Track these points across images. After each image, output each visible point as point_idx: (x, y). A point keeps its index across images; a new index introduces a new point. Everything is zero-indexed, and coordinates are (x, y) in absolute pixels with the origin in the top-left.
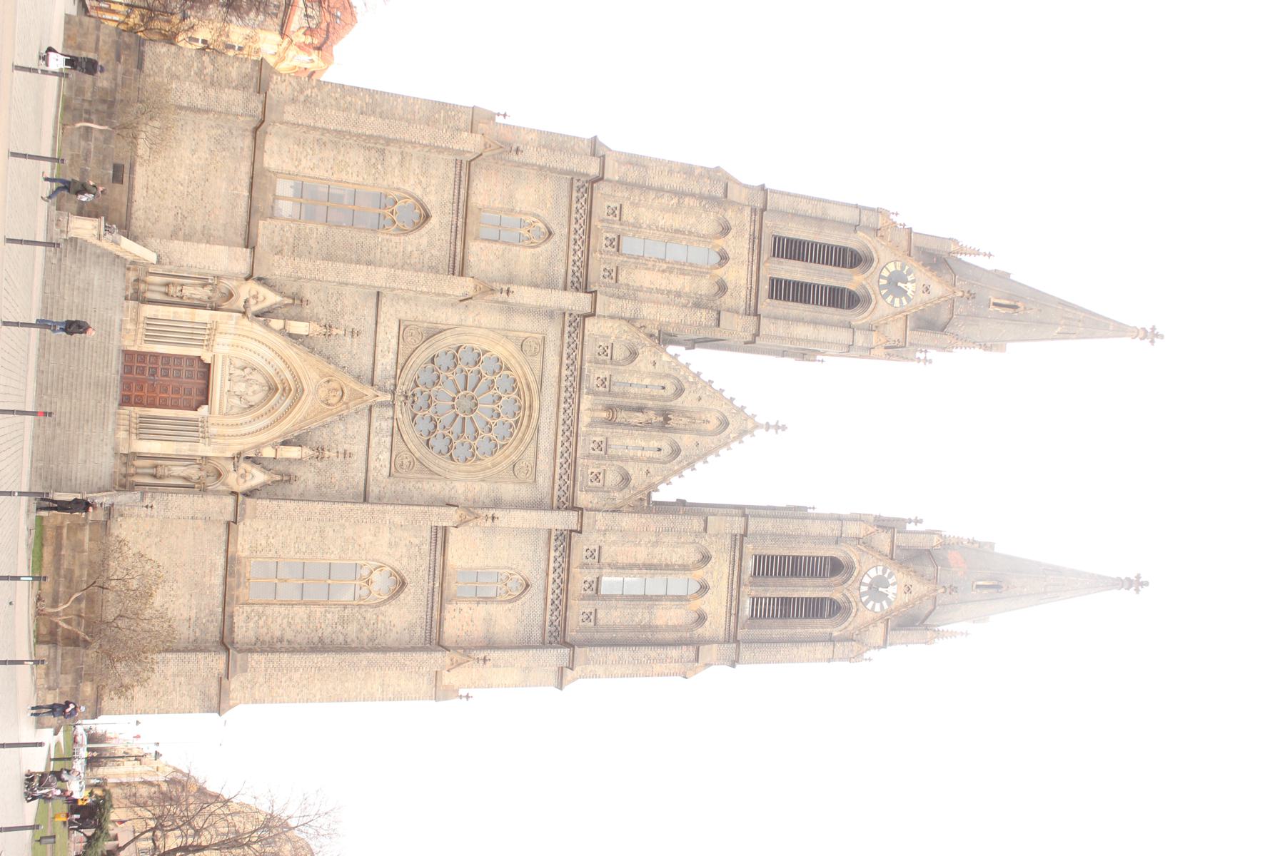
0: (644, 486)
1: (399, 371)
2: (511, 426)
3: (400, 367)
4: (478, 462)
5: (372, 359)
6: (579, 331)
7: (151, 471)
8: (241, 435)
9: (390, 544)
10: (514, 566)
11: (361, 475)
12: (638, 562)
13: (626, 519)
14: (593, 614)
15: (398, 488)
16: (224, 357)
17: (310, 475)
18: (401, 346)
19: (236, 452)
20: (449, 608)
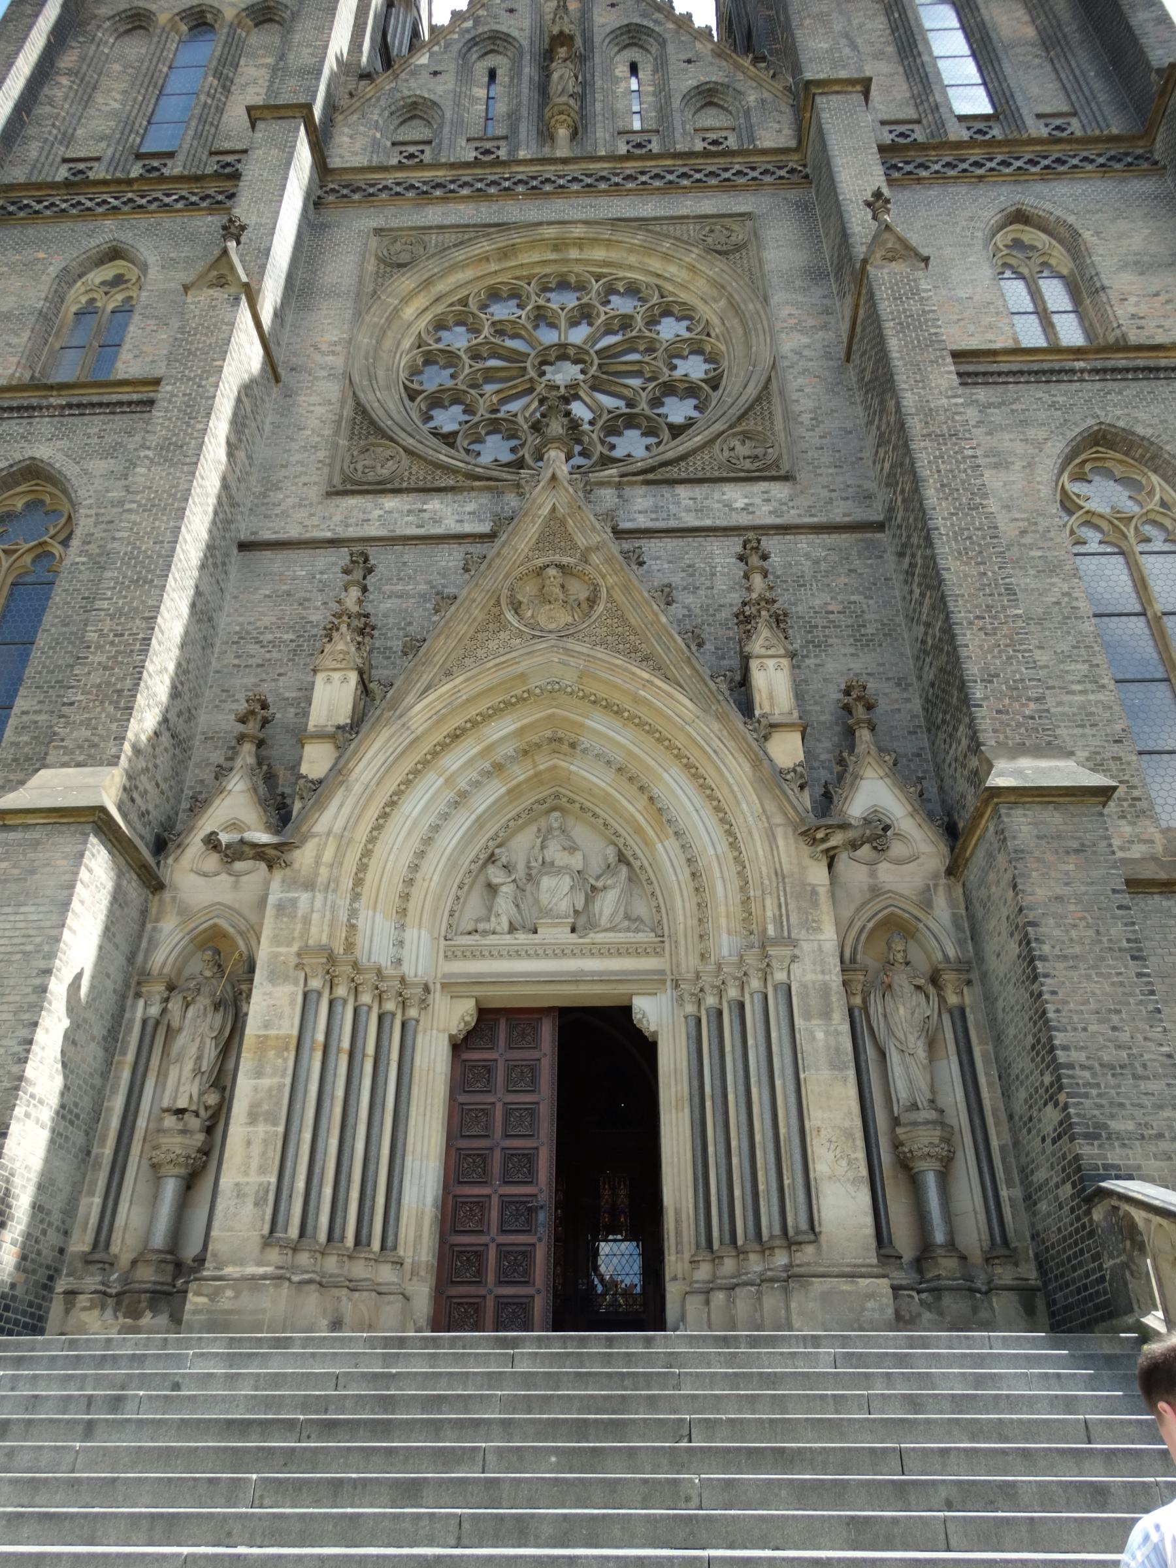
0: (724, 63)
1: (477, 483)
2: (610, 290)
3: (468, 483)
4: (718, 330)
5: (445, 547)
6: (359, 179)
7: (931, 1182)
8: (733, 845)
9: (996, 466)
10: (979, 234)
11: (803, 543)
12: (901, 70)
13: (811, 44)
14: (1049, 121)
15: (825, 460)
16: (451, 955)
17: (830, 667)
18: (405, 485)
19: (806, 850)
20: (1134, 338)
